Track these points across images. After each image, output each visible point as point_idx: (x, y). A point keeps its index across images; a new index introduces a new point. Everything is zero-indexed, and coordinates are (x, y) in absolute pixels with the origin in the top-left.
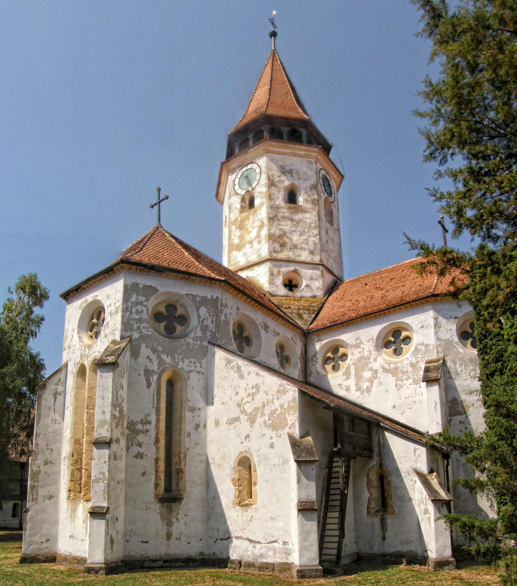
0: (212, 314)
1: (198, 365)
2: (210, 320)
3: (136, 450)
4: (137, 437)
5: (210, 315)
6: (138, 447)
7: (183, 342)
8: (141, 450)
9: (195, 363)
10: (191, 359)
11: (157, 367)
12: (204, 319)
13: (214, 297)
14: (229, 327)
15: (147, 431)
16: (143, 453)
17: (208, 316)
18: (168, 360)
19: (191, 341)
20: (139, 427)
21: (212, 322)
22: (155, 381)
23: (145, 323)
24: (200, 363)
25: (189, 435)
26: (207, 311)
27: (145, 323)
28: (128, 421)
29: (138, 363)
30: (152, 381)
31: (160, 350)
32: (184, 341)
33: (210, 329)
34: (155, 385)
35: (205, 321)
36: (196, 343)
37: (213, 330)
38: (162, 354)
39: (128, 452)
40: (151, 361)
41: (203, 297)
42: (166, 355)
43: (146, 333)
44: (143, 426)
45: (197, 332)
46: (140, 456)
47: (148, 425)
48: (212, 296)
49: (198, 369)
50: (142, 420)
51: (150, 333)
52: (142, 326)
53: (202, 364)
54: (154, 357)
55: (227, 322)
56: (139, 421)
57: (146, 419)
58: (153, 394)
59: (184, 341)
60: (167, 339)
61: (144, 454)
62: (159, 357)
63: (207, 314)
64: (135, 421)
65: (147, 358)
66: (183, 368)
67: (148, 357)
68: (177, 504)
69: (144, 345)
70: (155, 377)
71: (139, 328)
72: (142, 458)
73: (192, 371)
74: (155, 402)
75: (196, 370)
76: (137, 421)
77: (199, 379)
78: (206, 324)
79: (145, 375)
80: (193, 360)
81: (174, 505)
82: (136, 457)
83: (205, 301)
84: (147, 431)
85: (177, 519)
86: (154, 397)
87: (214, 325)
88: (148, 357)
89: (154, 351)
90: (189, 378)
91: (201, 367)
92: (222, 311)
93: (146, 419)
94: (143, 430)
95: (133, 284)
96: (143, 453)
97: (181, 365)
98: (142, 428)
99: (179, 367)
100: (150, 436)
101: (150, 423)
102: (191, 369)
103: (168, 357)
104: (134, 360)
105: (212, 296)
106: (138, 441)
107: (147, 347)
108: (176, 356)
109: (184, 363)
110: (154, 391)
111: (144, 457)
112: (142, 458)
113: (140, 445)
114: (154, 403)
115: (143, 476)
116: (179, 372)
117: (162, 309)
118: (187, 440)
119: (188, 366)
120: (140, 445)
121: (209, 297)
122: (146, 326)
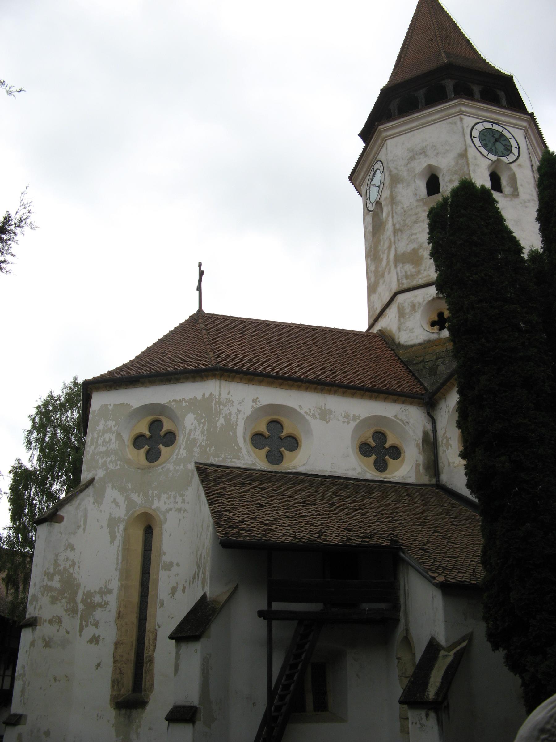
0: (203, 421)
1: (179, 499)
2: (200, 430)
3: (90, 631)
4: (94, 613)
5: (199, 423)
6: (94, 627)
7: (160, 471)
8: (97, 632)
9: (175, 497)
10: (170, 493)
11: (125, 512)
12: (190, 431)
13: (207, 395)
14: (235, 433)
15: (107, 603)
16: (99, 636)
17: (198, 425)
18: (137, 499)
19: (171, 467)
20: (97, 599)
21: (202, 432)
22: (121, 532)
23: (112, 456)
24: (182, 495)
25: (162, 605)
26: (196, 419)
27: (112, 456)
28: (84, 592)
29: (101, 511)
30: (117, 534)
31: (130, 487)
32: (162, 468)
33: (198, 444)
34: (120, 538)
35: (193, 433)
36: (177, 468)
37: (204, 443)
38: (132, 493)
39: (80, 635)
40: (117, 506)
41: (191, 399)
42: (137, 494)
43: (113, 468)
44: (102, 597)
45: (181, 452)
46: (95, 640)
47: (108, 595)
48: (204, 395)
49: (180, 505)
50: (101, 588)
51: (118, 467)
52: (109, 459)
53: (185, 498)
54: (121, 499)
55: (230, 426)
56: (97, 590)
57: (106, 586)
58: (118, 549)
59: (162, 468)
60: (139, 471)
61: (101, 638)
62: (127, 498)
63: (196, 423)
64: (92, 591)
65: (112, 502)
66: (158, 508)
67: (114, 501)
68: (139, 710)
69: (110, 485)
70: (122, 527)
71: (105, 464)
72: (97, 642)
73: (171, 509)
74: (120, 561)
75: (176, 507)
76: (95, 592)
77: (180, 520)
78: (193, 437)
79: (109, 526)
80: (172, 494)
81: (134, 712)
82: (91, 641)
83: (193, 404)
84: (107, 603)
85: (138, 735)
86: (118, 555)
87: (204, 435)
88: (114, 501)
89: (122, 490)
90: (166, 520)
91: (183, 501)
92: (220, 412)
93: (106, 586)
94: (101, 603)
95: (102, 407)
96: (99, 636)
97: (156, 504)
98: (100, 601)
99: (153, 507)
100: (110, 611)
101: (110, 592)
102: (171, 506)
103: (139, 497)
104: (97, 507)
105: (204, 395)
106: (94, 620)
107: (113, 487)
108: (150, 492)
109: (159, 500)
110: (119, 546)
111: (100, 642)
112: (97, 642)
113: (96, 625)
114: (117, 564)
115: (97, 669)
116: (153, 514)
117: (167, 426)
118: (159, 612)
119: (165, 503)
120: (96, 625)
121: (199, 397)
122: (114, 459)
